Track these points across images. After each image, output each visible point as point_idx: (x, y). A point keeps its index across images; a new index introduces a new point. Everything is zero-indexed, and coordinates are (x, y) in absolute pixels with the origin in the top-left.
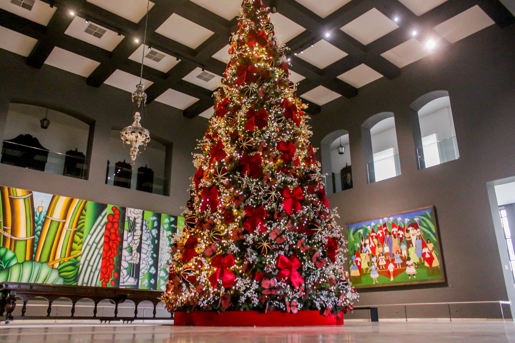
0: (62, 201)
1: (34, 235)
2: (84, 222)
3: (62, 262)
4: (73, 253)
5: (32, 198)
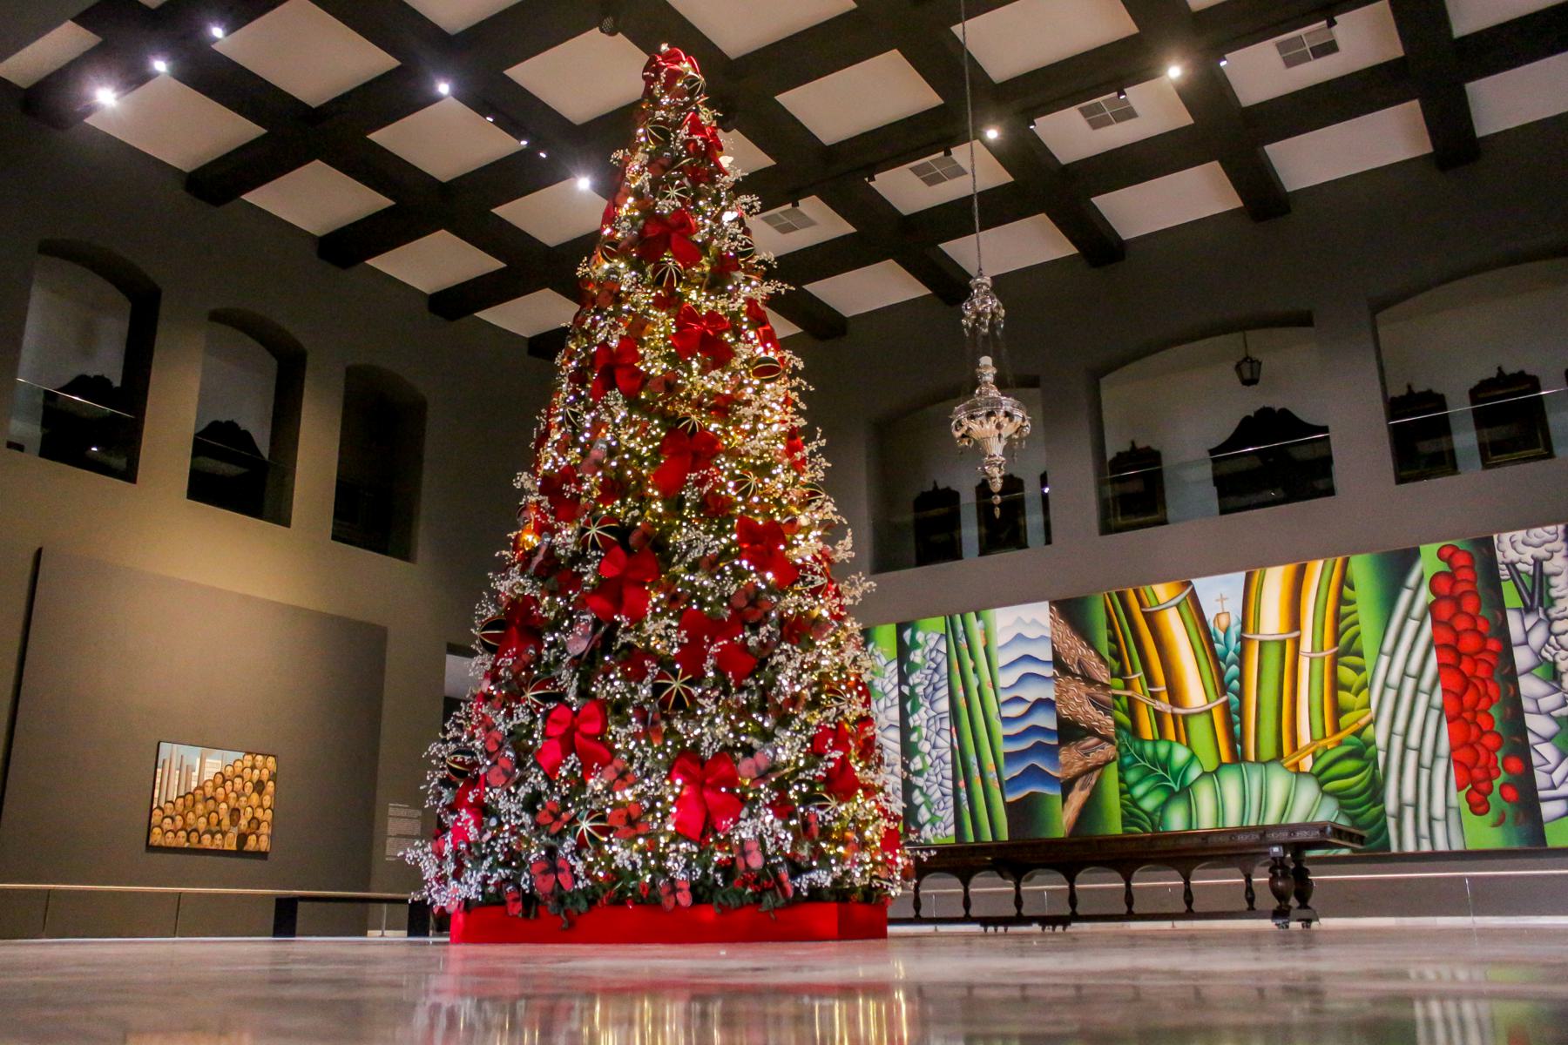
0: (1276, 580)
1: (1224, 693)
2: (1356, 623)
3: (1319, 753)
4: (1344, 720)
5: (1193, 596)
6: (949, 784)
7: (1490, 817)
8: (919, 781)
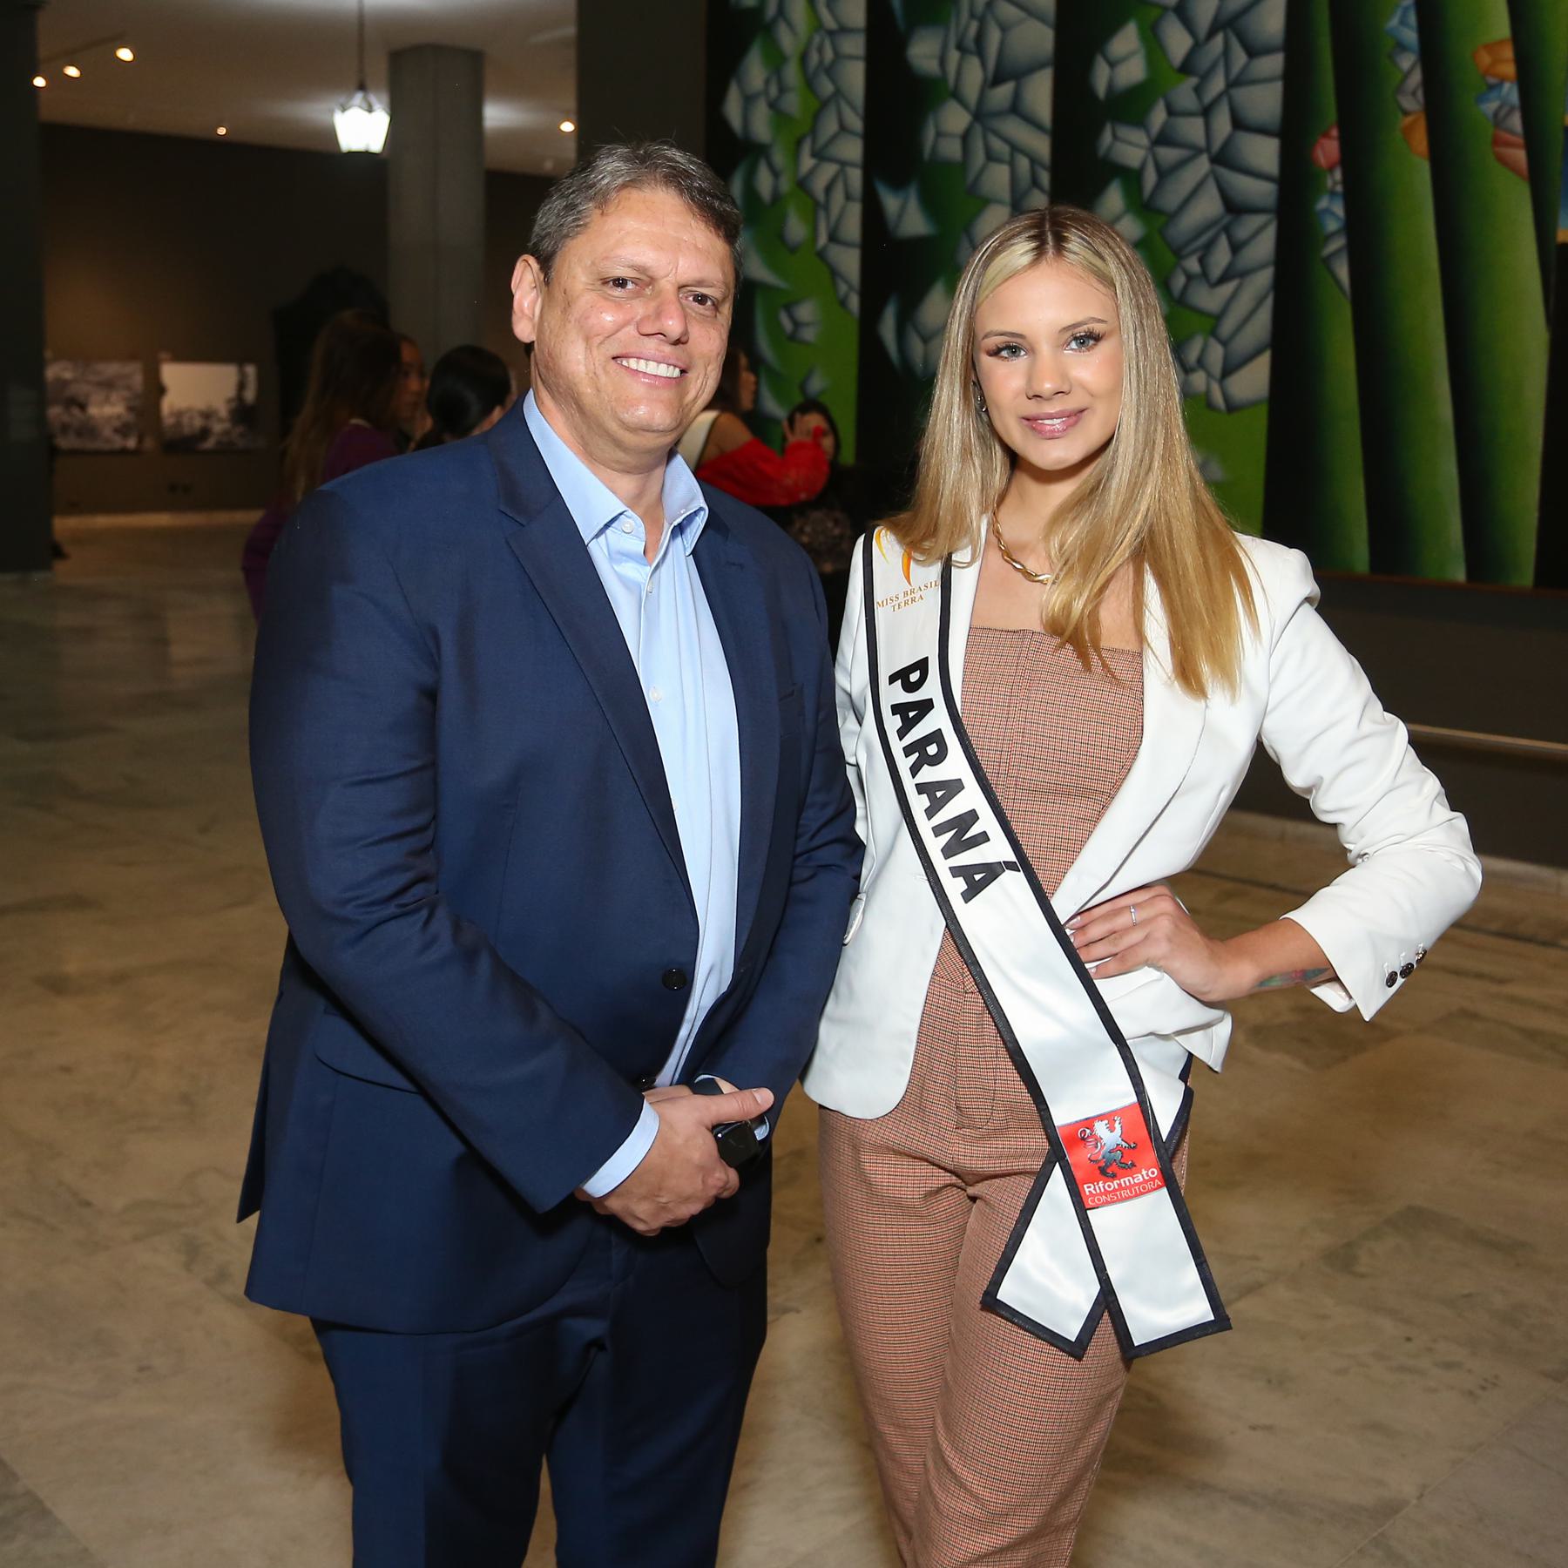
6: (1264, 153)
8: (1128, 146)
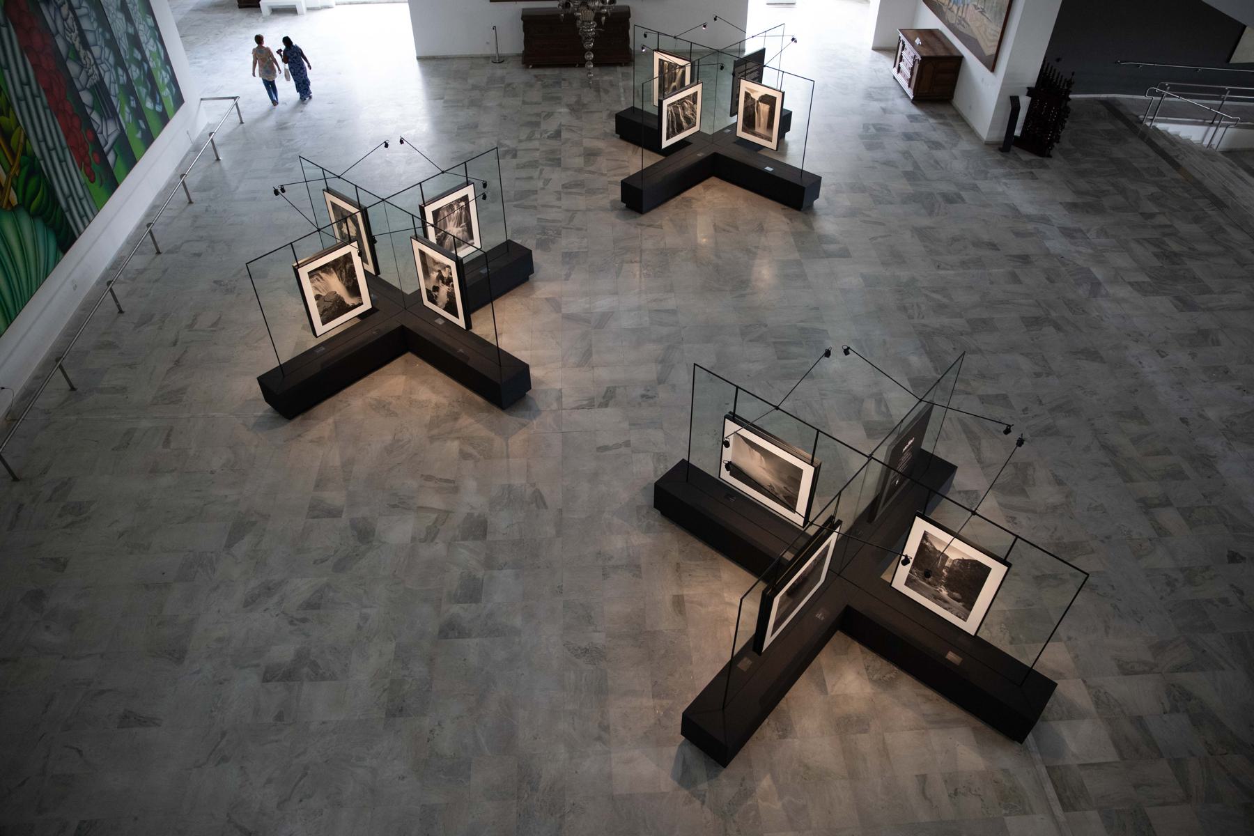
7: (97, 181)
